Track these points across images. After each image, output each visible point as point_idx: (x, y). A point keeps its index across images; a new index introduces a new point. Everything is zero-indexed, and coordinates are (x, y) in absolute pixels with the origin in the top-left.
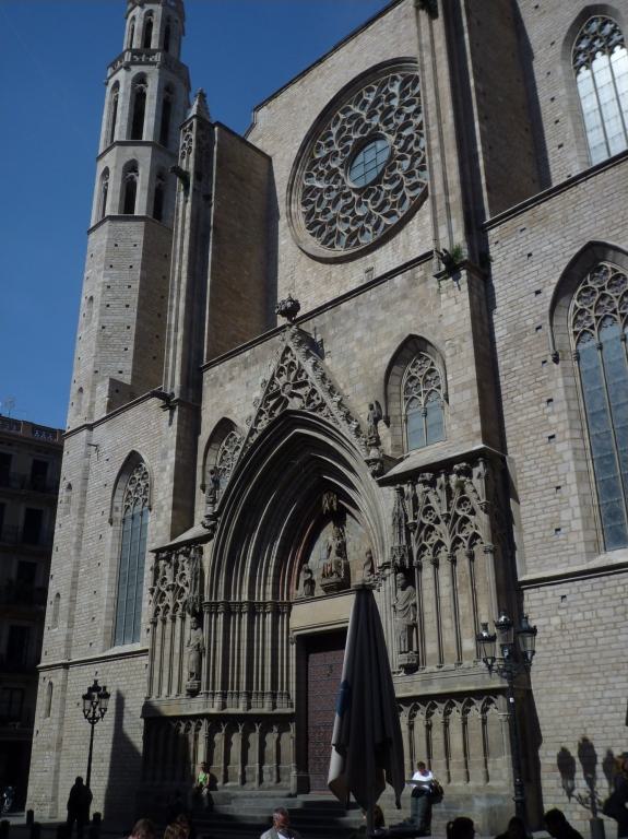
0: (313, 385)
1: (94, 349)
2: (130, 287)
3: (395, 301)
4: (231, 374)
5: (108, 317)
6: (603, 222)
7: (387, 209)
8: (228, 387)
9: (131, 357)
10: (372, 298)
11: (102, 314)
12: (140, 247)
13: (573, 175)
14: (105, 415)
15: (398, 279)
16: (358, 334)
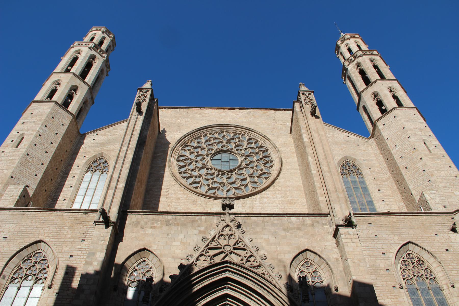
1: (16, 163)
2: (52, 143)
3: (291, 229)
4: (153, 224)
5: (33, 151)
6: (412, 235)
7: (235, 185)
8: (150, 231)
9: (38, 182)
10: (275, 222)
11: (30, 146)
12: (65, 127)
13: (390, 212)
14: (12, 207)
15: (293, 219)
16: (266, 237)
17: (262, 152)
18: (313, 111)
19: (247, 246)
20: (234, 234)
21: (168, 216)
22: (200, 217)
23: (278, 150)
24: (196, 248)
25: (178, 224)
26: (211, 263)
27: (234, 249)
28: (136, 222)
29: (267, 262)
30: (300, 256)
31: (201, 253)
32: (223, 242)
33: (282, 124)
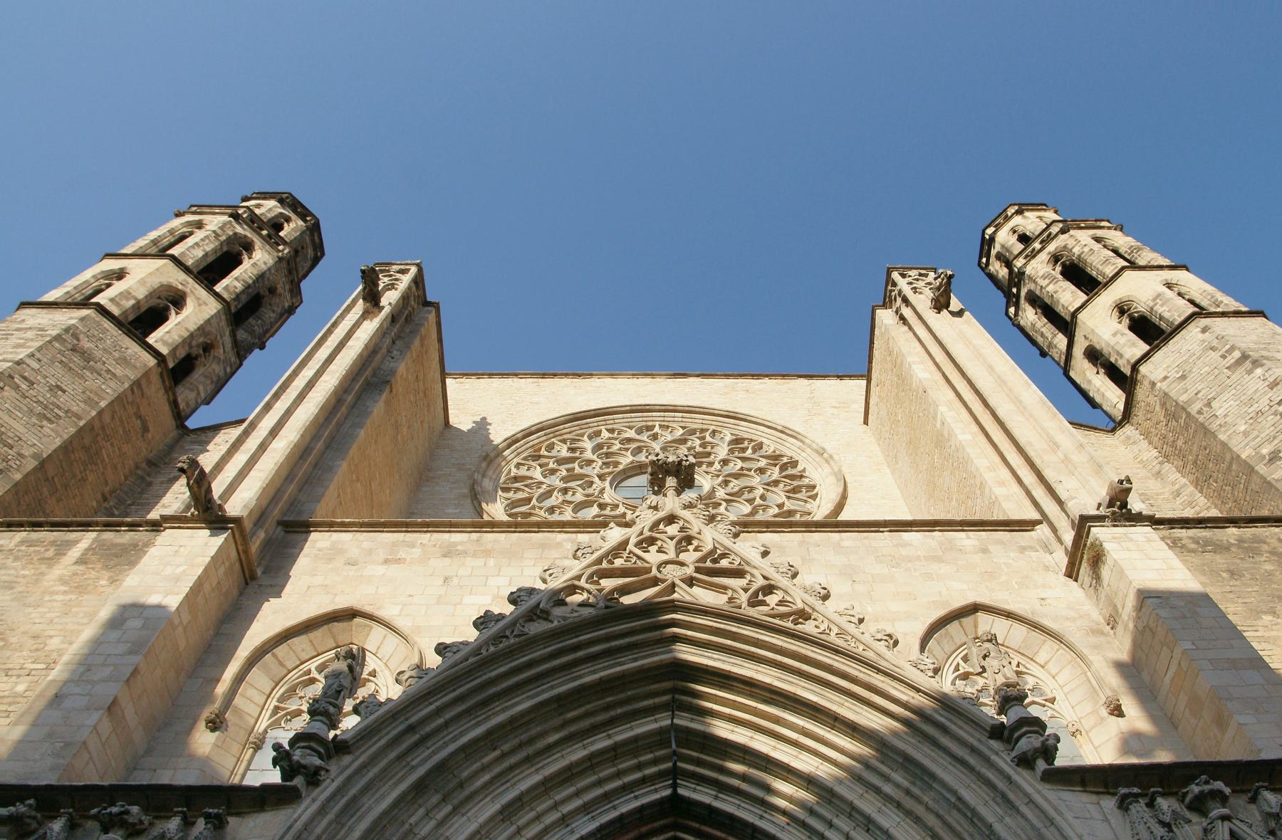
0: (765, 578)
8: (381, 570)
10: (846, 544)
17: (778, 467)
18: (941, 295)
19: (748, 564)
20: (698, 536)
21: (453, 535)
22: (569, 535)
23: (831, 457)
24: (551, 571)
25: (487, 553)
26: (607, 607)
27: (698, 570)
28: (330, 549)
29: (830, 607)
30: (954, 627)
31: (569, 583)
32: (653, 557)
33: (838, 405)
